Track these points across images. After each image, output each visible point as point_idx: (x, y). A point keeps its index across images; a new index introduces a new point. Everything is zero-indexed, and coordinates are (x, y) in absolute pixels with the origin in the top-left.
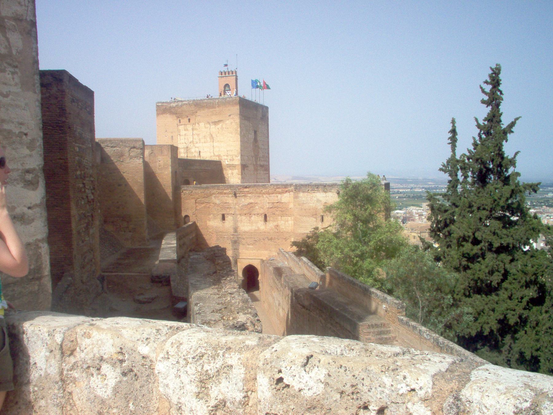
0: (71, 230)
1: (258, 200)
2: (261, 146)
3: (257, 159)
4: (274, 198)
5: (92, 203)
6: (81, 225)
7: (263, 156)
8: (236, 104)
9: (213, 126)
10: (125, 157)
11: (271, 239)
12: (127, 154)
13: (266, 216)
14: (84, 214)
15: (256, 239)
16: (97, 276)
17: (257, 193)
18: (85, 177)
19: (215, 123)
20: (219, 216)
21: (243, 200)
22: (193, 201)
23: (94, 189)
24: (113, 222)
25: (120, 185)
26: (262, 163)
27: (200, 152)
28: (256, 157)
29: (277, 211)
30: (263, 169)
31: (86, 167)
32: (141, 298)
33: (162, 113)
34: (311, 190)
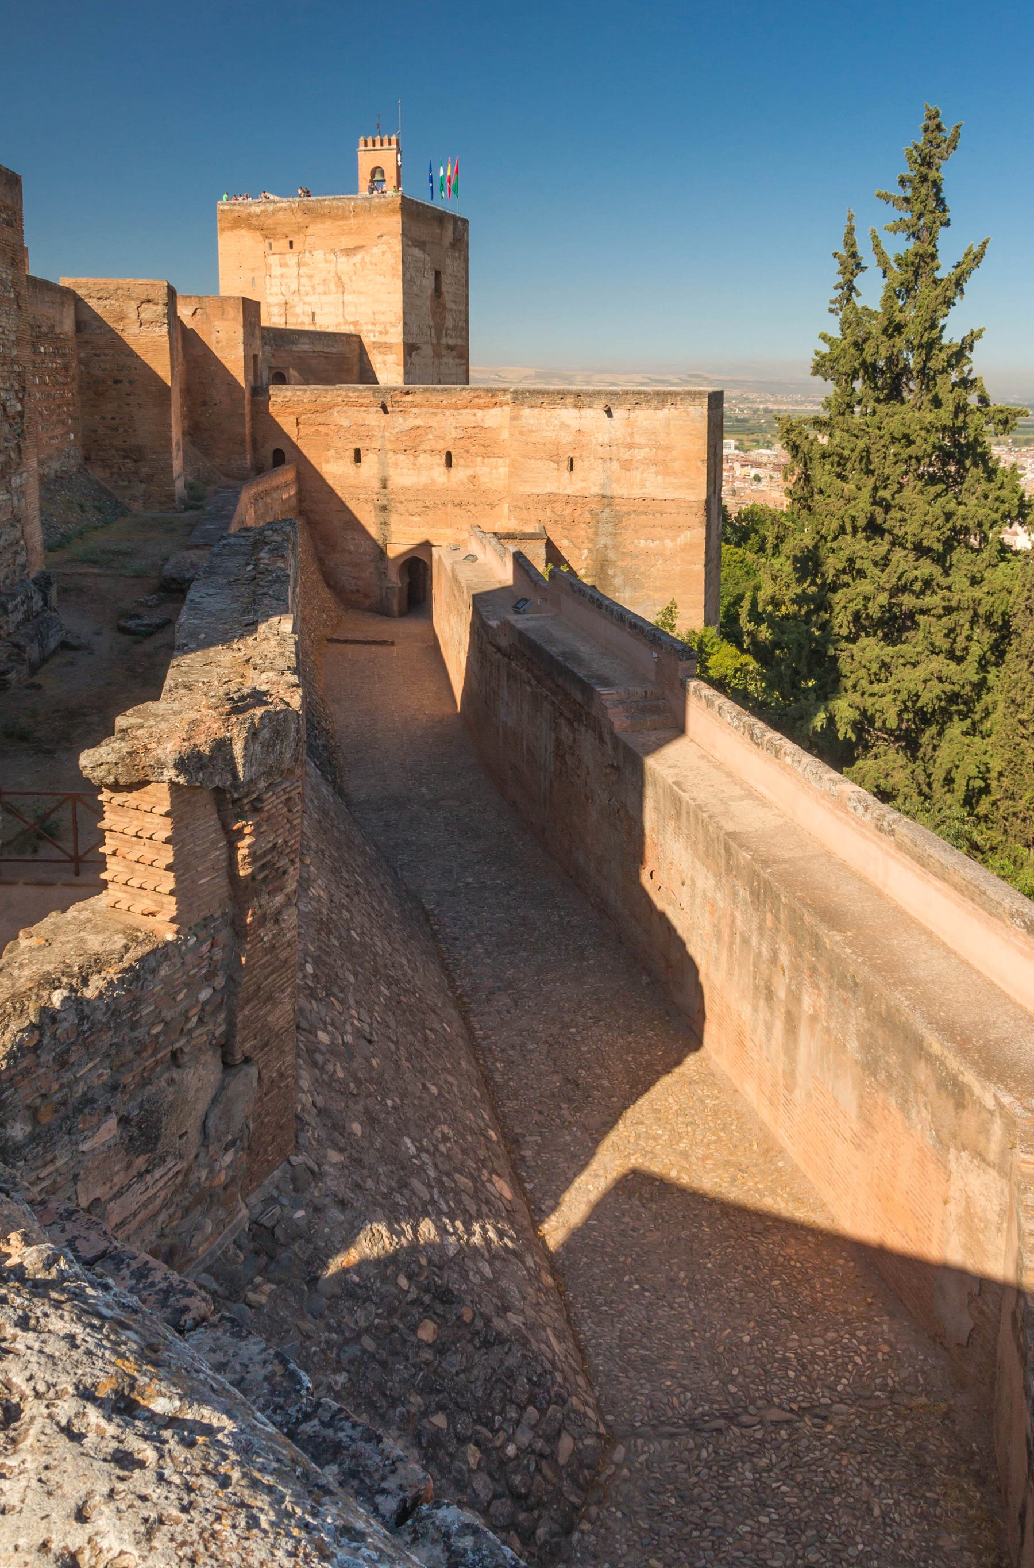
1: (433, 422)
2: (450, 305)
4: (467, 417)
8: (393, 211)
9: (344, 259)
10: (127, 321)
13: (449, 455)
16: (33, 576)
17: (431, 406)
19: (348, 252)
25: (116, 382)
26: (451, 342)
27: (313, 314)
28: (440, 329)
30: (454, 353)
32: (132, 623)
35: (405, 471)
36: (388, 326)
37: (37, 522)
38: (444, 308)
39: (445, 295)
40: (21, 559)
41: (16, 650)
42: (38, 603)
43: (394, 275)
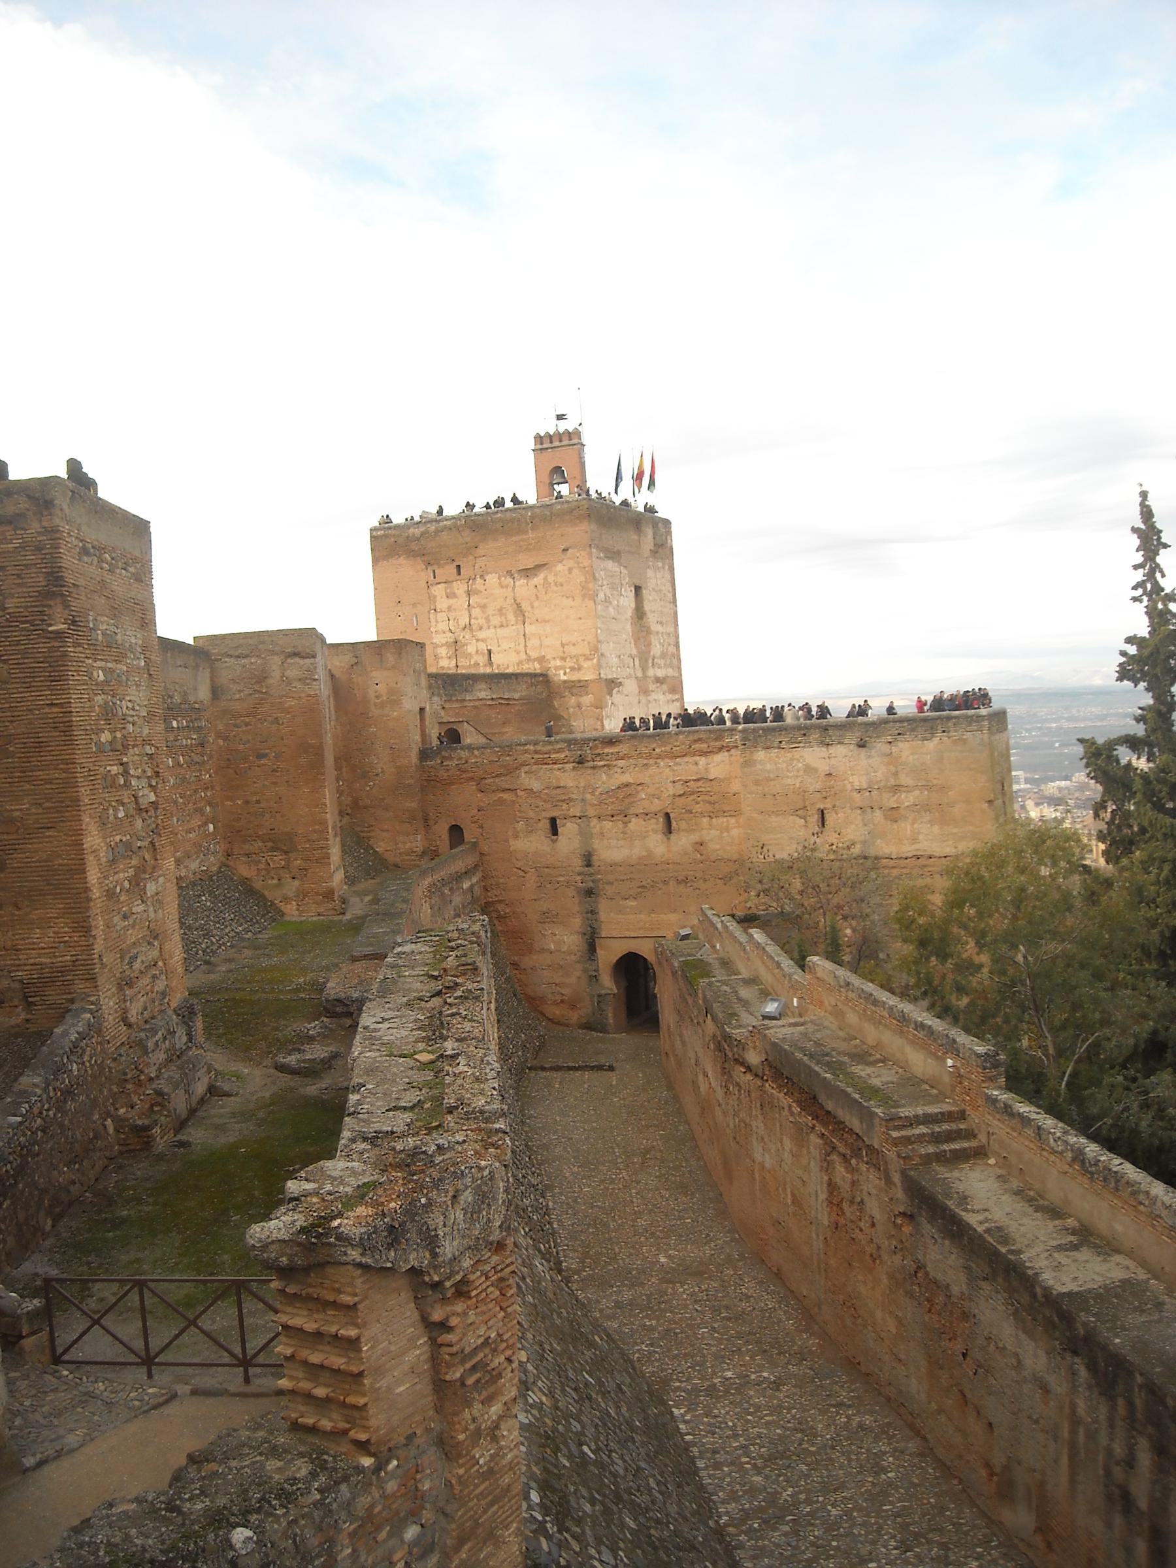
0: (87, 890)
2: (655, 627)
3: (647, 661)
4: (689, 767)
5: (152, 813)
6: (116, 873)
7: (662, 653)
9: (523, 581)
10: (271, 681)
11: (685, 881)
12: (277, 674)
13: (667, 815)
14: (128, 846)
15: (644, 883)
16: (174, 1005)
18: (126, 747)
19: (527, 573)
20: (540, 825)
21: (604, 777)
22: (472, 786)
23: (157, 774)
24: (248, 855)
26: (660, 673)
27: (490, 652)
28: (644, 658)
29: (698, 803)
30: (665, 687)
31: (131, 719)
33: (387, 557)
34: (787, 742)
35: (613, 842)
36: (581, 659)
37: (177, 937)
38: (649, 632)
39: (649, 615)
40: (161, 985)
41: (160, 1099)
42: (181, 1039)
43: (584, 596)
